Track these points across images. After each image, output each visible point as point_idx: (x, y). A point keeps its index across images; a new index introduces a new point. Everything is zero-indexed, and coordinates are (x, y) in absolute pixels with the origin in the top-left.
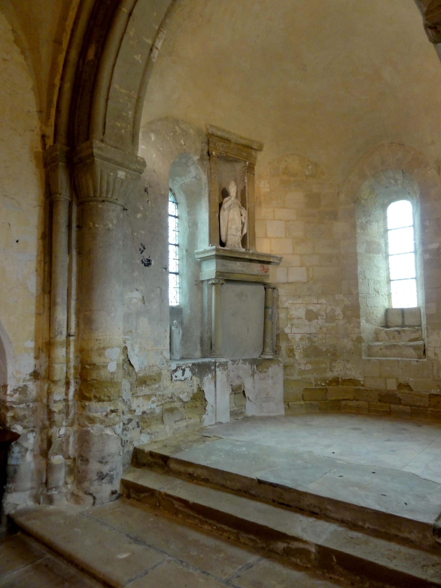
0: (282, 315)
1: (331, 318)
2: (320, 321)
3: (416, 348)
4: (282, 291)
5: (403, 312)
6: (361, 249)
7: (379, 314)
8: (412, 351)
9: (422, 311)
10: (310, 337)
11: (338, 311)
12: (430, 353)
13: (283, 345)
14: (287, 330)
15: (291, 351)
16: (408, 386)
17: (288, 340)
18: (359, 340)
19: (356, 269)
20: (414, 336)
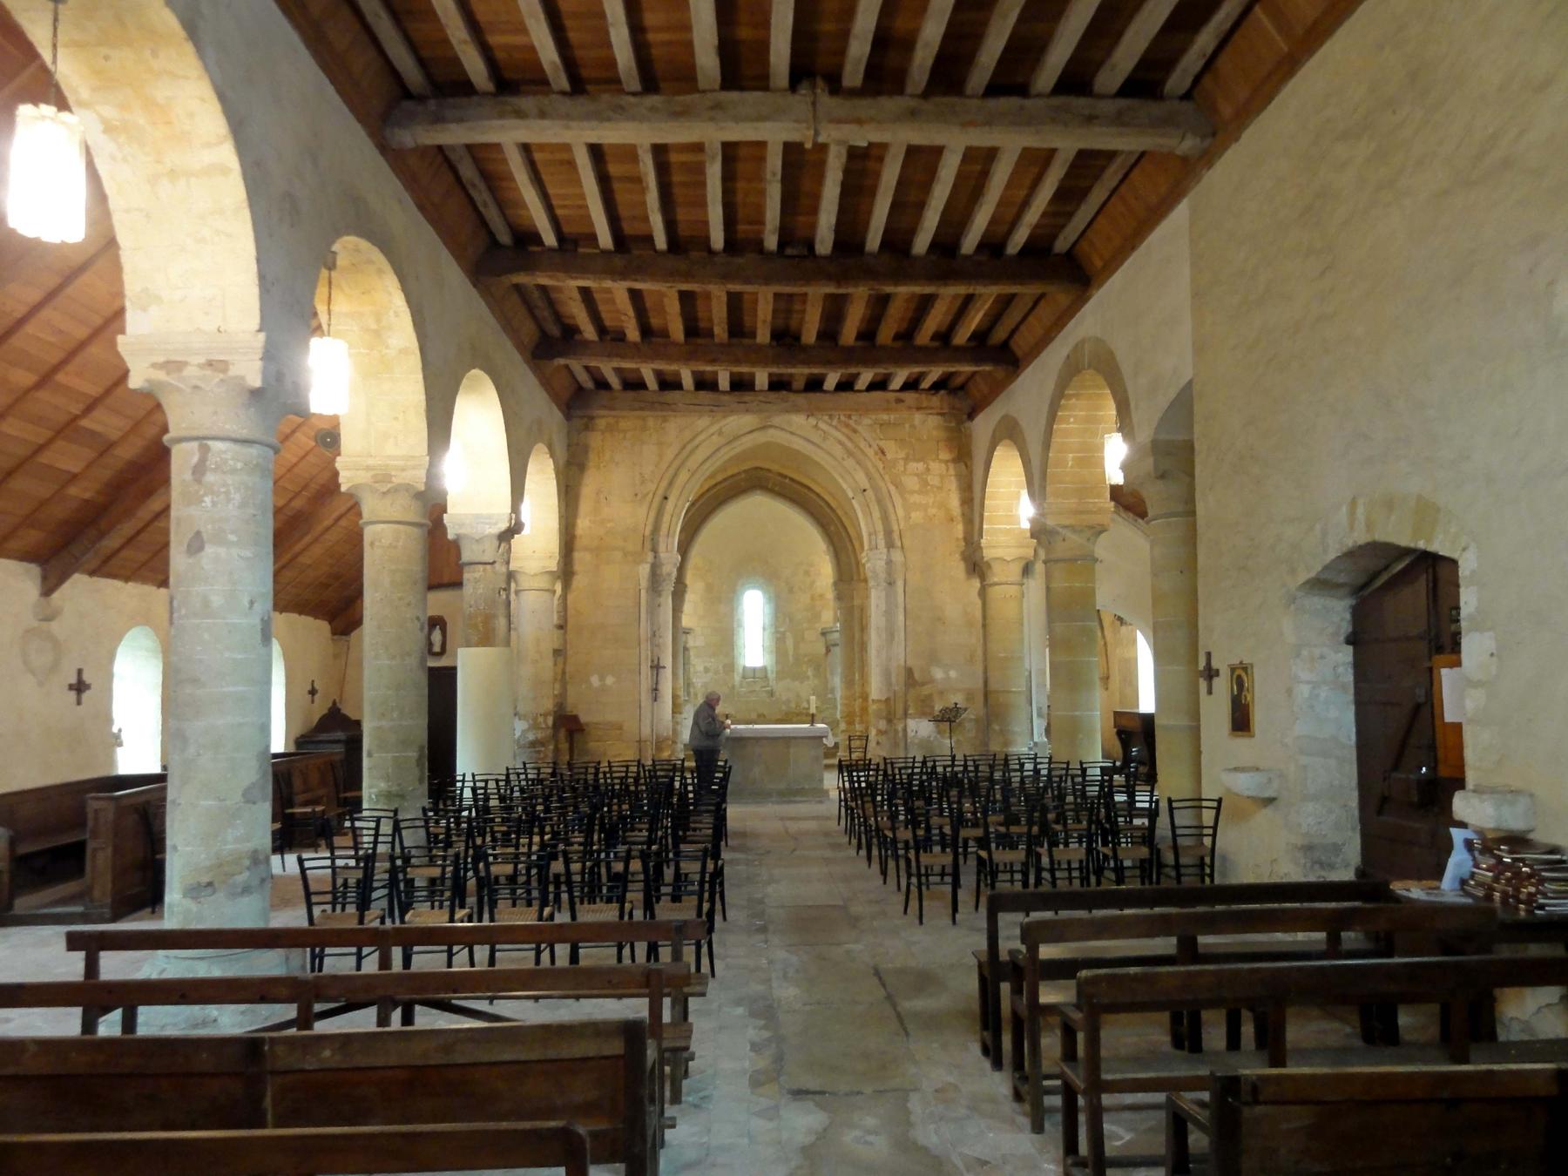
0: (692, 670)
1: (716, 672)
2: (710, 674)
3: (767, 692)
4: (692, 653)
5: (754, 670)
6: (735, 626)
7: (741, 671)
8: (764, 694)
9: (769, 668)
10: (705, 685)
11: (721, 667)
12: (777, 694)
13: (692, 690)
14: (694, 680)
15: (696, 695)
16: (764, 716)
17: (694, 688)
18: (733, 687)
19: (733, 639)
20: (764, 684)
